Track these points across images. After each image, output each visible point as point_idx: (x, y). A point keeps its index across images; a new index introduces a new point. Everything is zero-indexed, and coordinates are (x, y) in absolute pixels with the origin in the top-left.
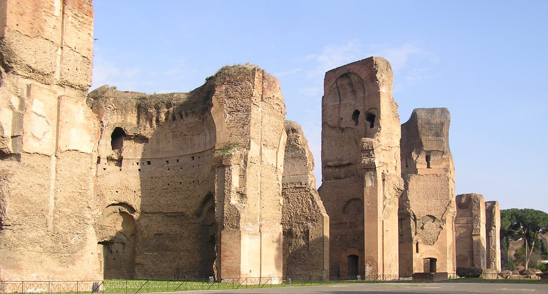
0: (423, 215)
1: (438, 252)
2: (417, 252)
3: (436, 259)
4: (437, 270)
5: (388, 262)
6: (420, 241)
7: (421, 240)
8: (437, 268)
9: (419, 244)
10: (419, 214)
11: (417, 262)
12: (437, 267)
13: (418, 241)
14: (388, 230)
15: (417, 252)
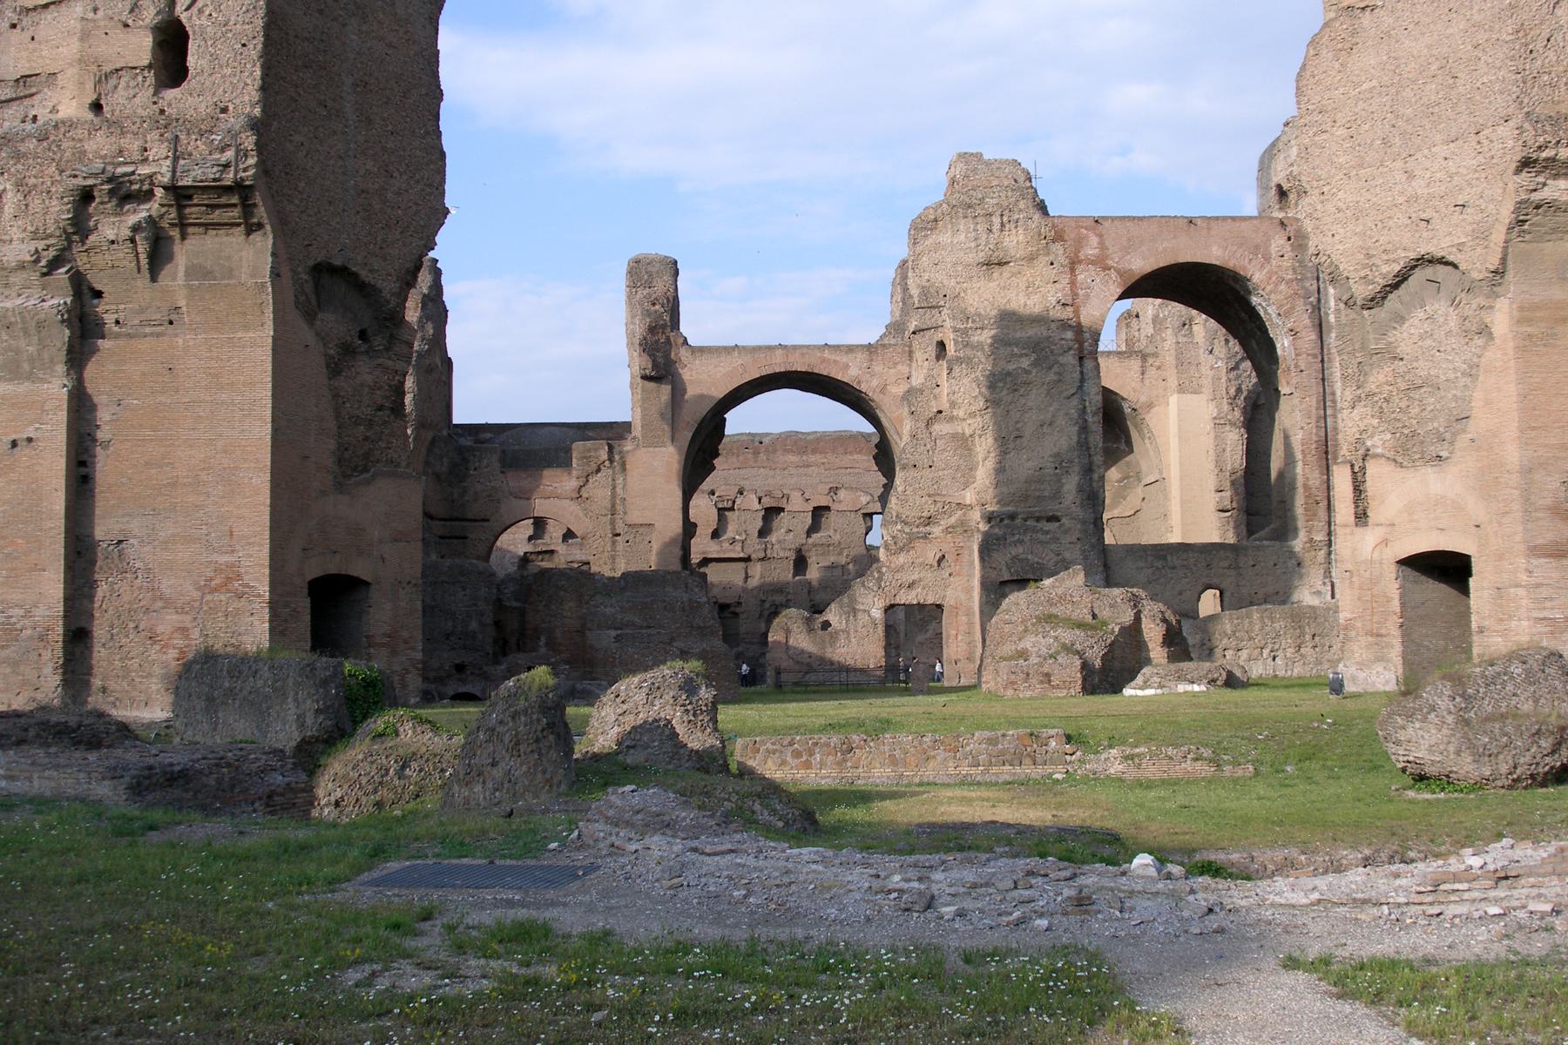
0: (1385, 269)
1: (1476, 509)
2: (1361, 517)
3: (1468, 557)
4: (1475, 638)
5: (28, 614)
6: (1377, 443)
7: (1389, 436)
8: (1474, 625)
9: (1372, 468)
10: (1365, 266)
11: (1361, 588)
12: (1473, 618)
13: (1369, 443)
14: (30, 440)
15: (1361, 517)
